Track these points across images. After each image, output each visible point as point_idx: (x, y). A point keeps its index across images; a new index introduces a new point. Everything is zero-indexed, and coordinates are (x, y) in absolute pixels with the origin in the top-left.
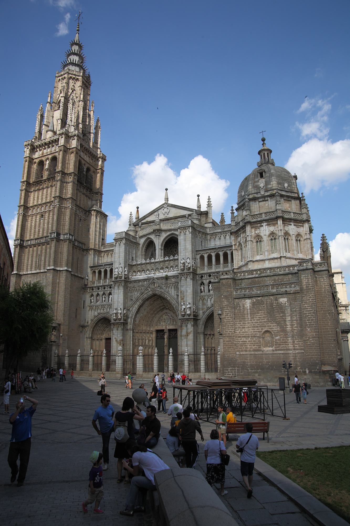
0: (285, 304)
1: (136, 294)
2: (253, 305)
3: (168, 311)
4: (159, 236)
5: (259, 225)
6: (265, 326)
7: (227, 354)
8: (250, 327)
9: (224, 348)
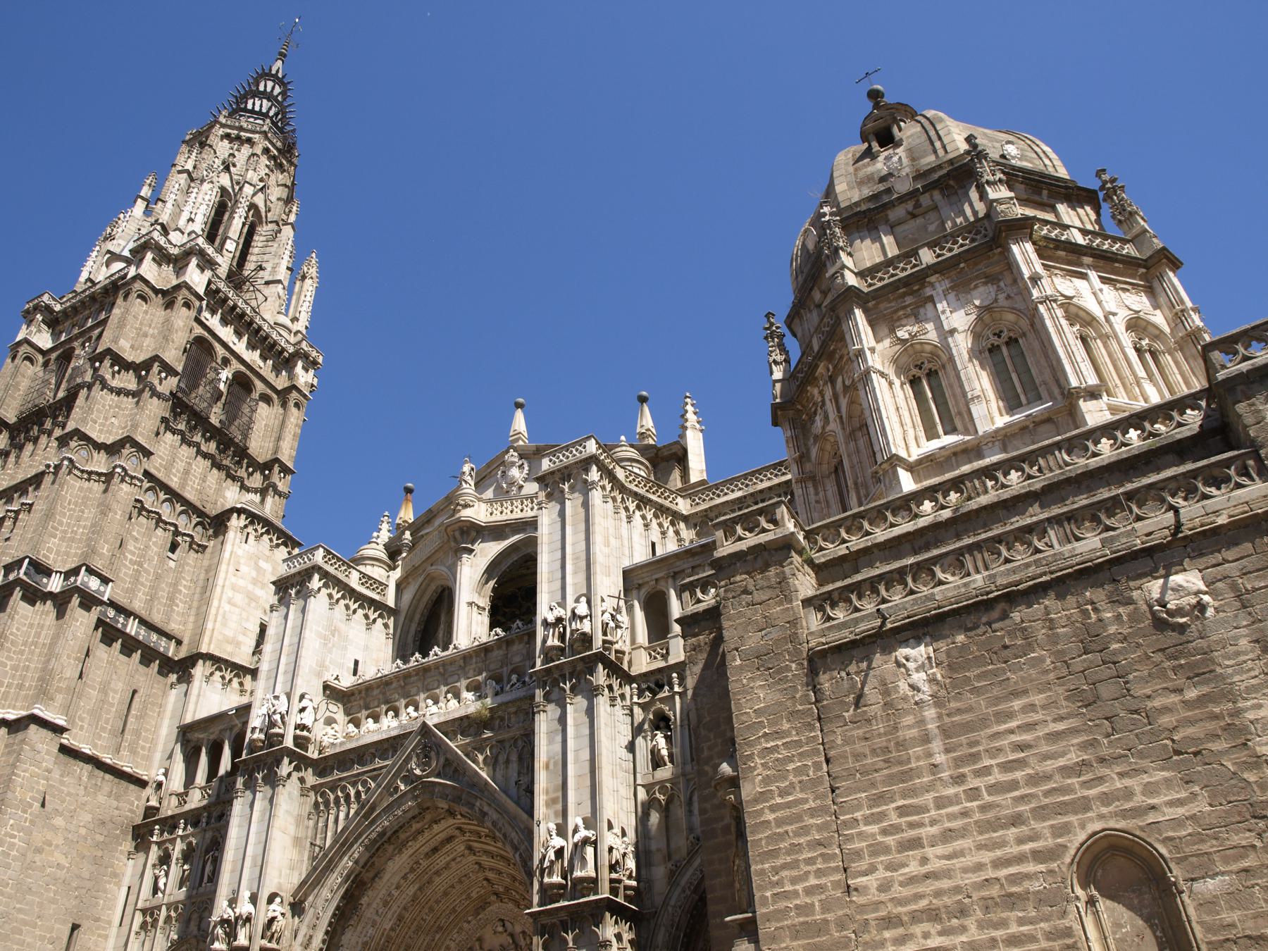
0: (1201, 607)
1: (342, 816)
4: (471, 551)
5: (909, 300)
6: (1084, 805)
8: (962, 833)
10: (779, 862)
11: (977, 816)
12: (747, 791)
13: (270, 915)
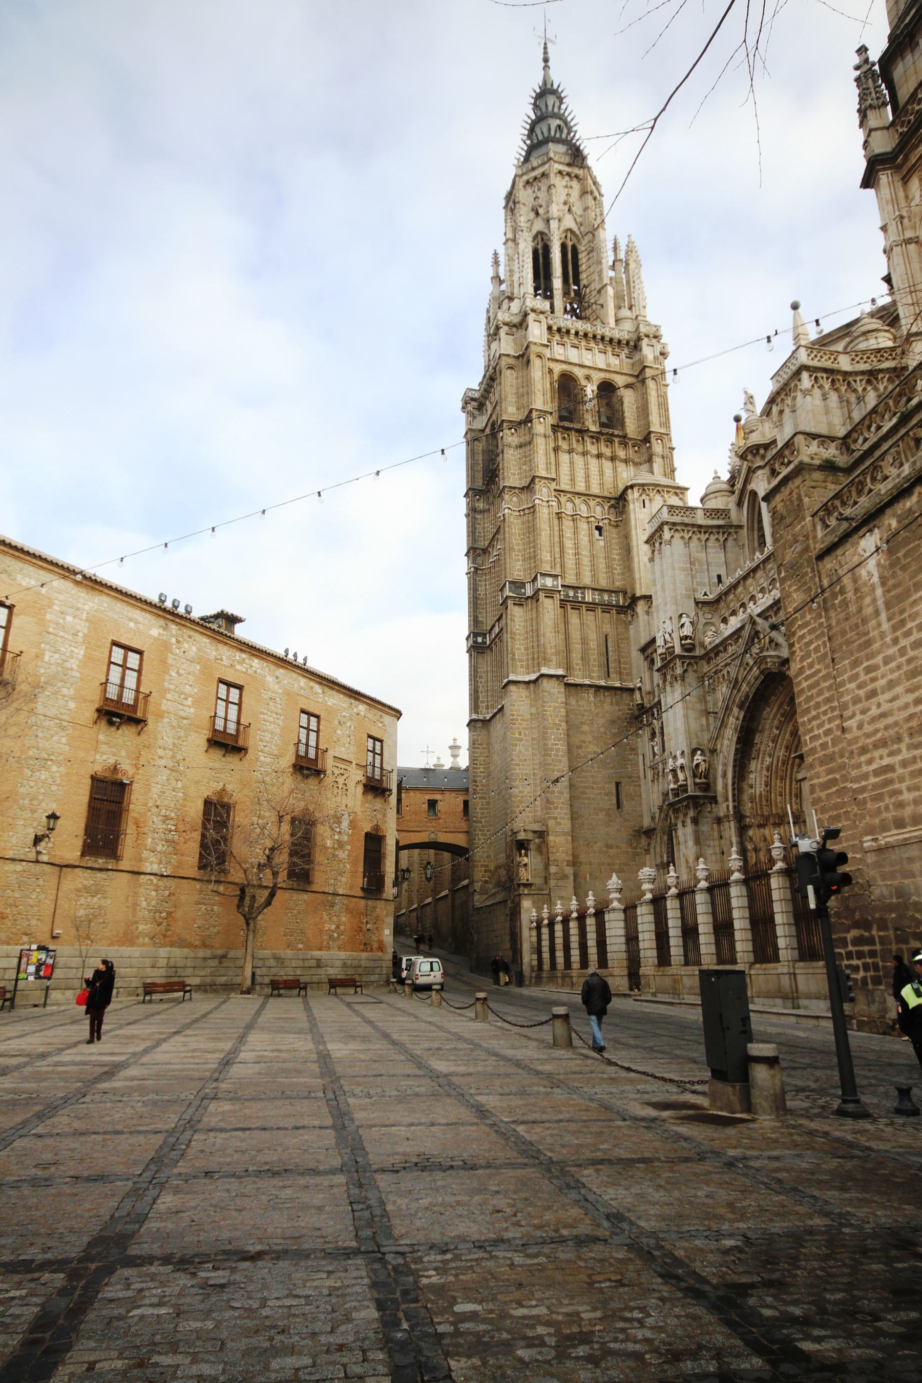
1: (723, 690)
2: (891, 552)
10: (810, 716)
11: (905, 668)
12: (794, 667)
13: (695, 762)
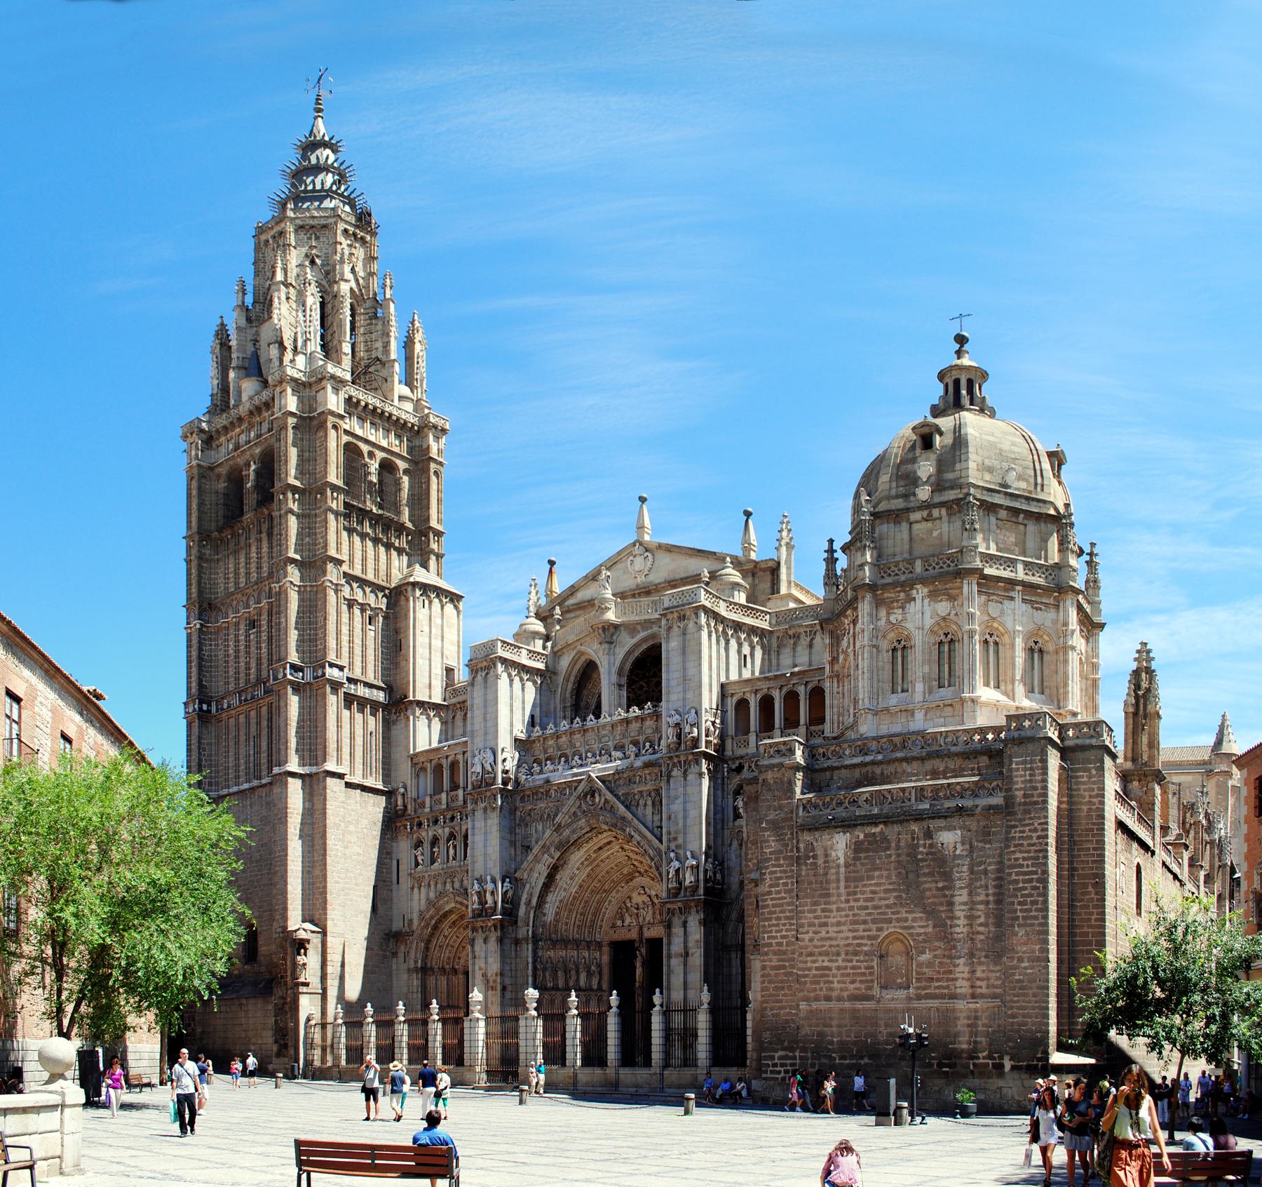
2: (856, 851)
3: (639, 880)
6: (889, 921)
7: (772, 1009)
8: (844, 924)
9: (762, 990)
12: (763, 888)
